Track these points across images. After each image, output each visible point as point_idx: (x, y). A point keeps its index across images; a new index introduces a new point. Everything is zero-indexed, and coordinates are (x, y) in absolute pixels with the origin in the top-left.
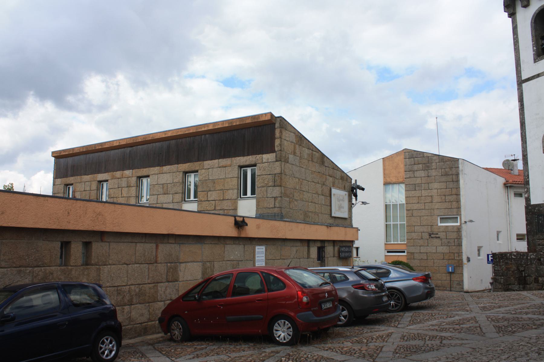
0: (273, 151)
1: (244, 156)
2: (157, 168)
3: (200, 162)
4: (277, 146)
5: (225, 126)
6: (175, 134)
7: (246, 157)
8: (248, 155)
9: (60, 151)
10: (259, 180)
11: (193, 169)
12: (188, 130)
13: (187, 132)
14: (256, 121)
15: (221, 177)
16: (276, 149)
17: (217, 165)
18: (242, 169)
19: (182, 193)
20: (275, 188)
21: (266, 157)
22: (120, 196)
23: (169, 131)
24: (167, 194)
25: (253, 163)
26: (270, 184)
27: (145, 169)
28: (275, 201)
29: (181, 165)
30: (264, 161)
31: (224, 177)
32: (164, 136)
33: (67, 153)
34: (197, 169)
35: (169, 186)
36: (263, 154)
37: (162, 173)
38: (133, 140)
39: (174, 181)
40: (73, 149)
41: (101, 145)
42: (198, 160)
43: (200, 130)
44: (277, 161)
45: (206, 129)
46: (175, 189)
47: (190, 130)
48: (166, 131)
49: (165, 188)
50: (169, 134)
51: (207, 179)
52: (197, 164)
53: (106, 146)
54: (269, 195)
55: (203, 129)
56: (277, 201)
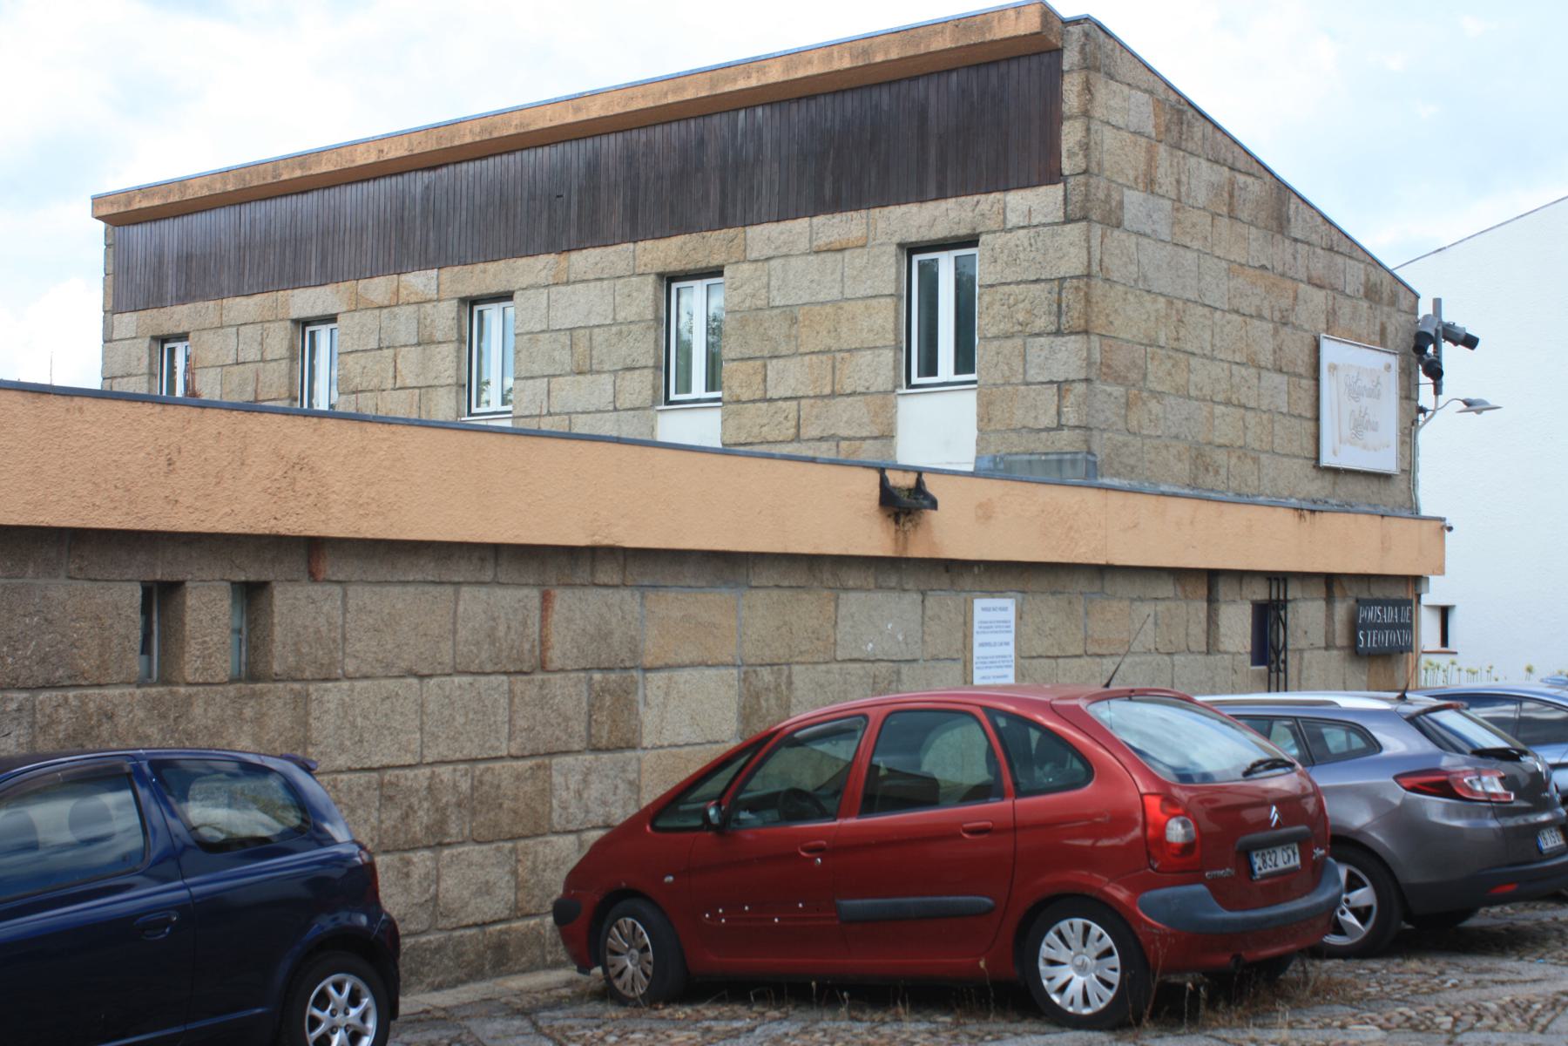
0: (1052, 175)
1: (921, 199)
2: (543, 259)
4: (1071, 154)
7: (930, 205)
8: (941, 195)
9: (126, 192)
10: (991, 304)
11: (702, 260)
12: (675, 92)
13: (671, 99)
14: (974, 39)
15: (821, 297)
16: (1067, 166)
17: (803, 245)
18: (916, 258)
19: (657, 367)
20: (1059, 340)
21: (1024, 203)
22: (389, 384)
23: (594, 94)
24: (591, 372)
25: (963, 231)
26: (1041, 323)
27: (492, 267)
28: (1061, 397)
29: (649, 244)
30: (1013, 219)
31: (835, 294)
33: (157, 202)
36: (1007, 190)
37: (567, 283)
39: (620, 318)
40: (182, 183)
41: (302, 166)
42: (724, 223)
44: (1068, 220)
45: (753, 82)
46: (624, 351)
47: (683, 89)
48: (581, 96)
49: (583, 344)
50: (595, 111)
51: (760, 303)
52: (717, 237)
53: (324, 169)
54: (1033, 374)
55: (742, 84)
56: (1070, 399)
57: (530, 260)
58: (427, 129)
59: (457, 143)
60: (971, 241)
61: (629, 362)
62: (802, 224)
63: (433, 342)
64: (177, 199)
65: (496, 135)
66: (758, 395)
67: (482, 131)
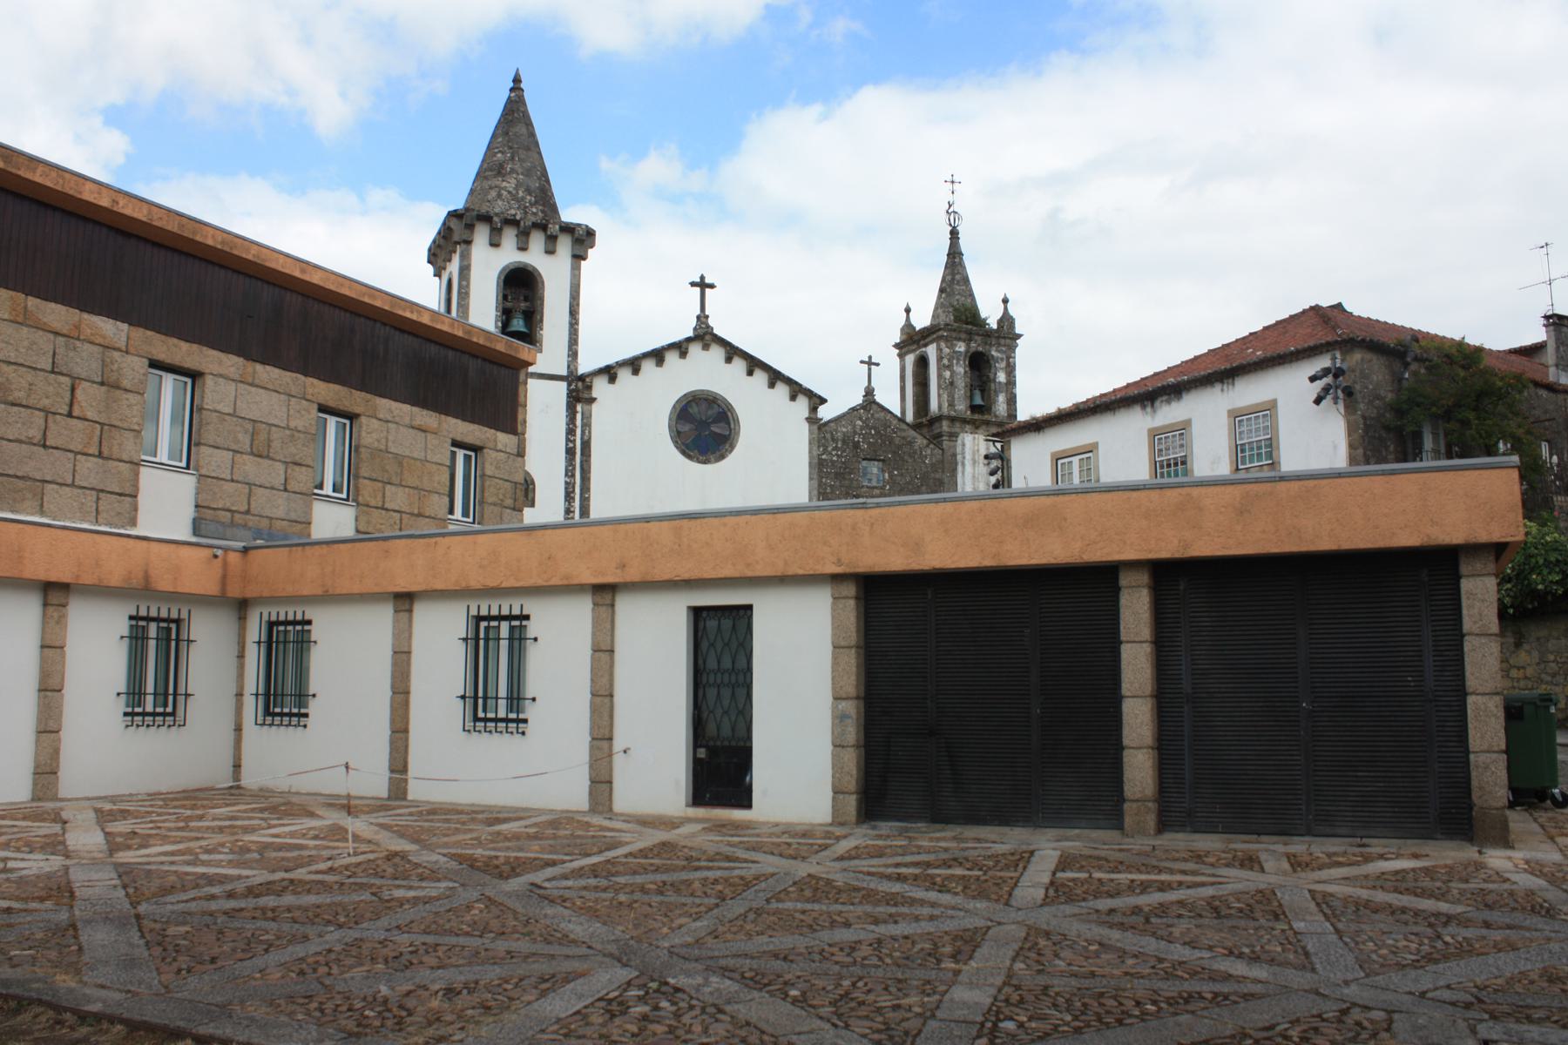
3: (369, 396)
6: (332, 288)
12: (371, 296)
13: (366, 300)
17: (407, 420)
19: (357, 477)
22: (64, 409)
24: (268, 457)
25: (478, 443)
27: (185, 346)
29: (315, 381)
31: (422, 455)
32: (297, 274)
34: (357, 410)
35: (276, 434)
37: (251, 385)
38: (181, 226)
39: (292, 424)
42: (363, 387)
43: (400, 312)
45: (414, 317)
46: (293, 450)
48: (307, 263)
49: (263, 436)
50: (316, 279)
55: (408, 315)
57: (222, 356)
58: (169, 211)
59: (198, 238)
60: (477, 449)
61: (297, 458)
63: (118, 388)
65: (235, 252)
67: (223, 243)
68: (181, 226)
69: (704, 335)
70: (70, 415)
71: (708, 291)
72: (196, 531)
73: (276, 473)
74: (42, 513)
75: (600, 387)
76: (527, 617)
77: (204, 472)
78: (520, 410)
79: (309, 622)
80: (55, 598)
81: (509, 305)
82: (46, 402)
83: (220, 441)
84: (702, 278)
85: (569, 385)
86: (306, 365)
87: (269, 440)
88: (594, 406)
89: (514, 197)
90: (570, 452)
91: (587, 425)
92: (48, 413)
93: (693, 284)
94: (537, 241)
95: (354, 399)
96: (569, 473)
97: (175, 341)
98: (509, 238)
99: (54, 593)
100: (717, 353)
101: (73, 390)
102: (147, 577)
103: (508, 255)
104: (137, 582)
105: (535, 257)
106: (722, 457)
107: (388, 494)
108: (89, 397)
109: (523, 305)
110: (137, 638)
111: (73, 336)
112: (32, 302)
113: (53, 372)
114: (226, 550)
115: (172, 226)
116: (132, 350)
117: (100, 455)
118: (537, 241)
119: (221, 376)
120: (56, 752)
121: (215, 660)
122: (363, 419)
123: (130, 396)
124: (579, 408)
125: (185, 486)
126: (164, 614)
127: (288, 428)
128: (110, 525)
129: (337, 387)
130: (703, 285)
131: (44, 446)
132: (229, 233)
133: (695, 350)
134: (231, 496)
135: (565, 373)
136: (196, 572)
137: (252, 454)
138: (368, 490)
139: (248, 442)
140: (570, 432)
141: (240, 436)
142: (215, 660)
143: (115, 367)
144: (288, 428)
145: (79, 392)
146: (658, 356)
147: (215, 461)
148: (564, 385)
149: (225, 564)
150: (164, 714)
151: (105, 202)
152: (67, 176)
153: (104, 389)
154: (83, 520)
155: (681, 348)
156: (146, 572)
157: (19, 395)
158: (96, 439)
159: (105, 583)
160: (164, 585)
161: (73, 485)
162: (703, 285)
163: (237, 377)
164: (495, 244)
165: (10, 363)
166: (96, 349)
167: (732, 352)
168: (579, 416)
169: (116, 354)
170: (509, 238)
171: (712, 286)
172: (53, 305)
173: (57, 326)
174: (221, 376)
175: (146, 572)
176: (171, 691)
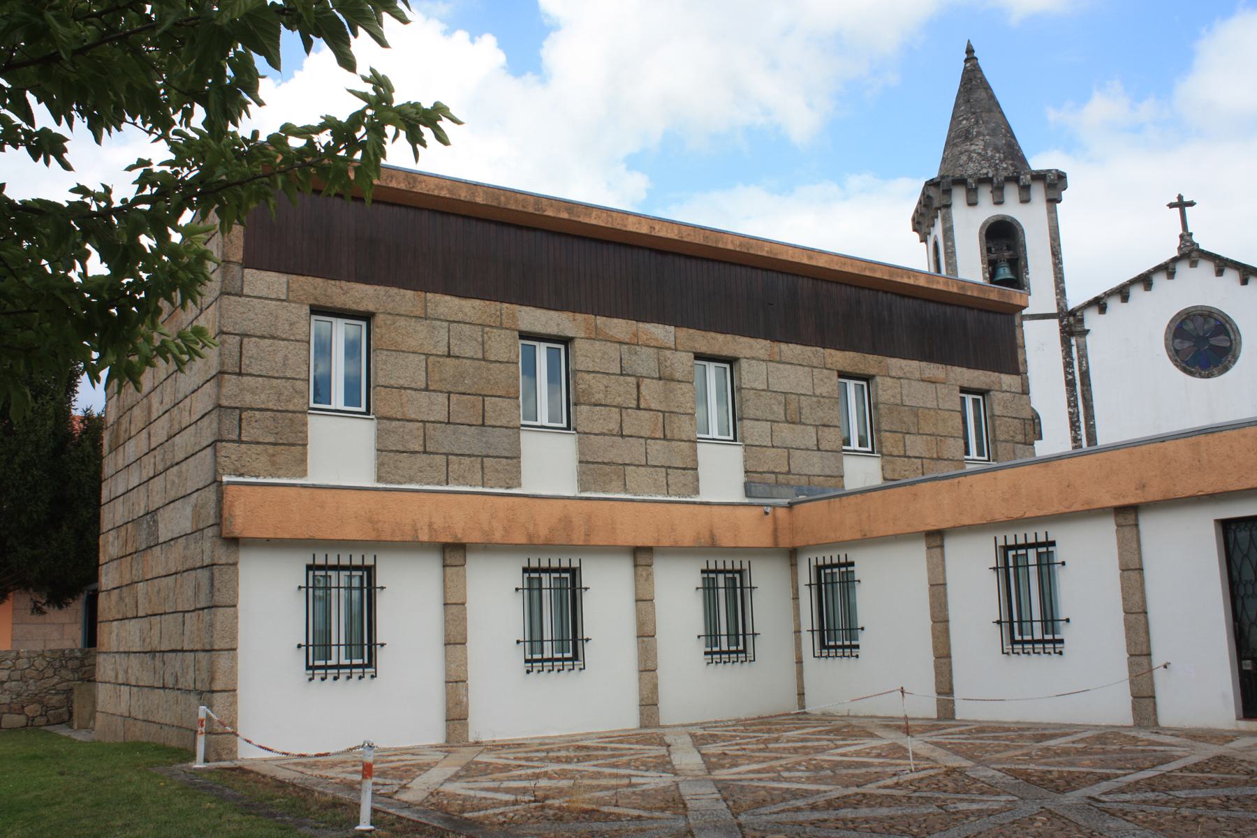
5: (951, 289)
6: (837, 268)
8: (977, 368)
13: (868, 273)
17: (917, 375)
19: (879, 431)
24: (801, 423)
25: (984, 387)
27: (720, 337)
29: (832, 351)
31: (934, 405)
32: (805, 261)
34: (872, 371)
35: (805, 402)
37: (780, 362)
38: (706, 238)
39: (818, 392)
42: (874, 351)
43: (899, 280)
45: (911, 282)
46: (821, 414)
48: (813, 250)
49: (794, 406)
50: (821, 262)
55: (906, 280)
58: (695, 227)
59: (720, 246)
60: (983, 393)
62: (915, 364)
63: (673, 380)
64: (403, 186)
65: (752, 251)
66: (902, 453)
67: (740, 245)
68: (706, 238)
69: (1190, 253)
70: (638, 408)
71: (1187, 209)
72: (748, 493)
73: (807, 436)
74: (626, 491)
75: (1092, 319)
76: (1053, 544)
77: (748, 442)
78: (1019, 351)
79: (852, 564)
80: (642, 559)
81: (993, 256)
82: (619, 400)
83: (759, 414)
84: (1180, 197)
85: (1061, 321)
86: (823, 338)
87: (800, 408)
88: (1088, 338)
89: (984, 157)
90: (1070, 384)
91: (1083, 356)
92: (621, 408)
93: (1171, 206)
94: (1011, 193)
95: (868, 363)
96: (1072, 403)
97: (713, 334)
98: (985, 195)
99: (641, 555)
100: (1206, 268)
101: (638, 387)
102: (712, 536)
103: (987, 211)
104: (705, 540)
105: (1012, 209)
106: (1226, 369)
107: (908, 443)
108: (651, 390)
109: (1007, 254)
110: (709, 588)
111: (633, 343)
112: (601, 320)
113: (621, 374)
114: (774, 507)
115: (698, 239)
116: (679, 347)
117: (665, 438)
118: (1011, 193)
119: (753, 358)
120: (655, 687)
121: (774, 602)
122: (878, 379)
123: (682, 385)
124: (1073, 341)
125: (735, 454)
126: (729, 567)
127: (815, 395)
128: (679, 495)
129: (852, 354)
130: (1181, 205)
131: (622, 436)
132: (744, 236)
133: (1183, 269)
134: (772, 460)
135: (1055, 310)
136: (752, 529)
137: (787, 421)
138: (889, 441)
139: (782, 412)
140: (1068, 365)
141: (775, 407)
142: (774, 602)
143: (668, 364)
144: (815, 395)
145: (642, 388)
146: (1145, 280)
147: (756, 431)
148: (1056, 322)
149: (775, 519)
150: (737, 652)
151: (644, 230)
152: (614, 214)
153: (661, 382)
154: (657, 493)
155: (1168, 269)
156: (711, 531)
157: (599, 397)
158: (660, 425)
159: (680, 544)
160: (727, 541)
161: (647, 465)
162: (1181, 205)
163: (766, 357)
164: (972, 203)
165: (589, 372)
166: (652, 350)
167: (1222, 264)
168: (1074, 349)
169: (668, 353)
170: (985, 195)
171: (1191, 204)
172: (615, 320)
173: (621, 336)
174: (753, 358)
175: (711, 531)
176: (741, 632)
